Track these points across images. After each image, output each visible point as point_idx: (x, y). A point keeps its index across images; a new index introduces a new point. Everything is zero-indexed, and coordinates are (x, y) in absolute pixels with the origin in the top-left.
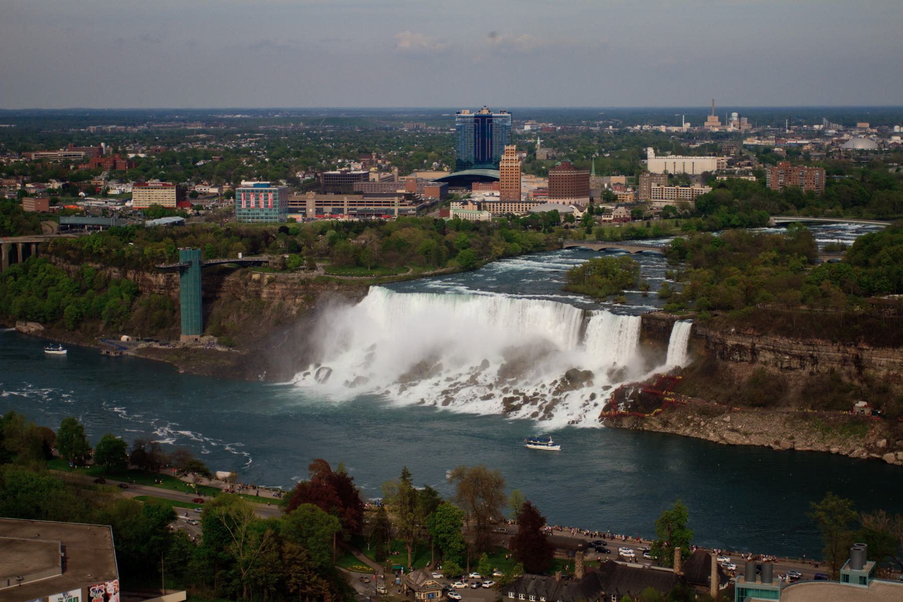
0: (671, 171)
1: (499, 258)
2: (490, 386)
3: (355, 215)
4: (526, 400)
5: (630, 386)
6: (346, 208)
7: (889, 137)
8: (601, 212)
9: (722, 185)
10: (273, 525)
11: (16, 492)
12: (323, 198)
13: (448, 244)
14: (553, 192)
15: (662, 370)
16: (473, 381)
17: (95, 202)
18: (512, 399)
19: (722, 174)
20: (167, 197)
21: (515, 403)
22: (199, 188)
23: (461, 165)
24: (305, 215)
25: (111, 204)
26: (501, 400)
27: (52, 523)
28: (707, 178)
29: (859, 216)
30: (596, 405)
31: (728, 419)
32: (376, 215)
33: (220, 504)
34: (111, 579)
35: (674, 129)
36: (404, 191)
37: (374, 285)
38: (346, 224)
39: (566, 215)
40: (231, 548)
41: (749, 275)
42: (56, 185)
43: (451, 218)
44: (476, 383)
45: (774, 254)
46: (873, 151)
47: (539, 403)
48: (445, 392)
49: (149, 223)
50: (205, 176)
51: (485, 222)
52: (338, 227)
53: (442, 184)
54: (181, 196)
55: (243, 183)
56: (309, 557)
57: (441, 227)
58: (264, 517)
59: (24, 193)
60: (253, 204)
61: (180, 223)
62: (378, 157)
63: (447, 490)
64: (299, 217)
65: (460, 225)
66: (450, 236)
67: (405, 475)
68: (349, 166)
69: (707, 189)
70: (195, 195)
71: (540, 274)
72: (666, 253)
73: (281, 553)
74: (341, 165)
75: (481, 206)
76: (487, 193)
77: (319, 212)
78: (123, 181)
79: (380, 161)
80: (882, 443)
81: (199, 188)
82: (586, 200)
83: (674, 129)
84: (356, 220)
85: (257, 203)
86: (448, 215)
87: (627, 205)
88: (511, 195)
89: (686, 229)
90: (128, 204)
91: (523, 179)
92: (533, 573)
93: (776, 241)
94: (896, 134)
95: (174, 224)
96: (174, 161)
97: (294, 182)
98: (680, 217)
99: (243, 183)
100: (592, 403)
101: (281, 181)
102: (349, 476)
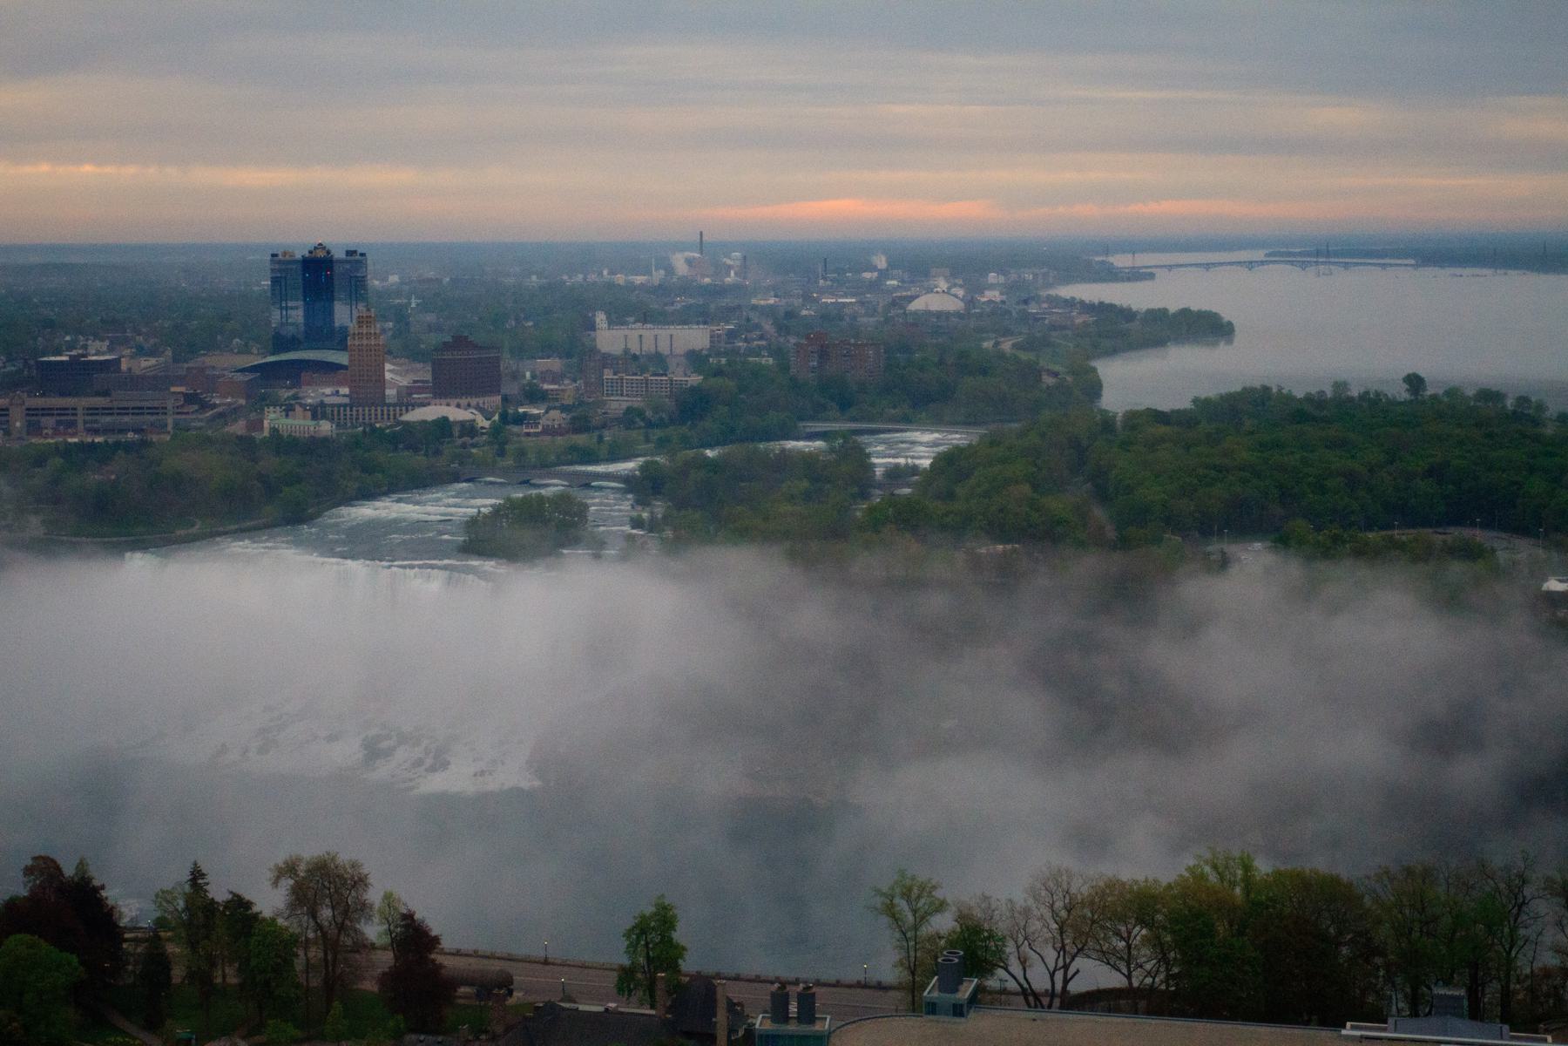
0: (634, 348)
1: (349, 500)
3: (96, 432)
6: (80, 419)
7: (981, 292)
8: (521, 419)
9: (719, 372)
12: (40, 402)
14: (443, 388)
19: (719, 354)
21: (385, 744)
28: (695, 359)
29: (937, 422)
32: (136, 431)
35: (639, 279)
38: (81, 447)
39: (462, 423)
41: (766, 519)
45: (805, 484)
46: (958, 314)
51: (325, 440)
52: (67, 451)
53: (250, 376)
63: (270, 901)
65: (282, 444)
67: (197, 875)
68: (85, 347)
69: (695, 379)
72: (630, 484)
74: (70, 348)
75: (318, 412)
76: (328, 391)
77: (34, 428)
79: (140, 339)
87: (564, 409)
89: (662, 444)
91: (388, 366)
93: (808, 460)
94: (992, 287)
98: (650, 425)
102: (96, 883)
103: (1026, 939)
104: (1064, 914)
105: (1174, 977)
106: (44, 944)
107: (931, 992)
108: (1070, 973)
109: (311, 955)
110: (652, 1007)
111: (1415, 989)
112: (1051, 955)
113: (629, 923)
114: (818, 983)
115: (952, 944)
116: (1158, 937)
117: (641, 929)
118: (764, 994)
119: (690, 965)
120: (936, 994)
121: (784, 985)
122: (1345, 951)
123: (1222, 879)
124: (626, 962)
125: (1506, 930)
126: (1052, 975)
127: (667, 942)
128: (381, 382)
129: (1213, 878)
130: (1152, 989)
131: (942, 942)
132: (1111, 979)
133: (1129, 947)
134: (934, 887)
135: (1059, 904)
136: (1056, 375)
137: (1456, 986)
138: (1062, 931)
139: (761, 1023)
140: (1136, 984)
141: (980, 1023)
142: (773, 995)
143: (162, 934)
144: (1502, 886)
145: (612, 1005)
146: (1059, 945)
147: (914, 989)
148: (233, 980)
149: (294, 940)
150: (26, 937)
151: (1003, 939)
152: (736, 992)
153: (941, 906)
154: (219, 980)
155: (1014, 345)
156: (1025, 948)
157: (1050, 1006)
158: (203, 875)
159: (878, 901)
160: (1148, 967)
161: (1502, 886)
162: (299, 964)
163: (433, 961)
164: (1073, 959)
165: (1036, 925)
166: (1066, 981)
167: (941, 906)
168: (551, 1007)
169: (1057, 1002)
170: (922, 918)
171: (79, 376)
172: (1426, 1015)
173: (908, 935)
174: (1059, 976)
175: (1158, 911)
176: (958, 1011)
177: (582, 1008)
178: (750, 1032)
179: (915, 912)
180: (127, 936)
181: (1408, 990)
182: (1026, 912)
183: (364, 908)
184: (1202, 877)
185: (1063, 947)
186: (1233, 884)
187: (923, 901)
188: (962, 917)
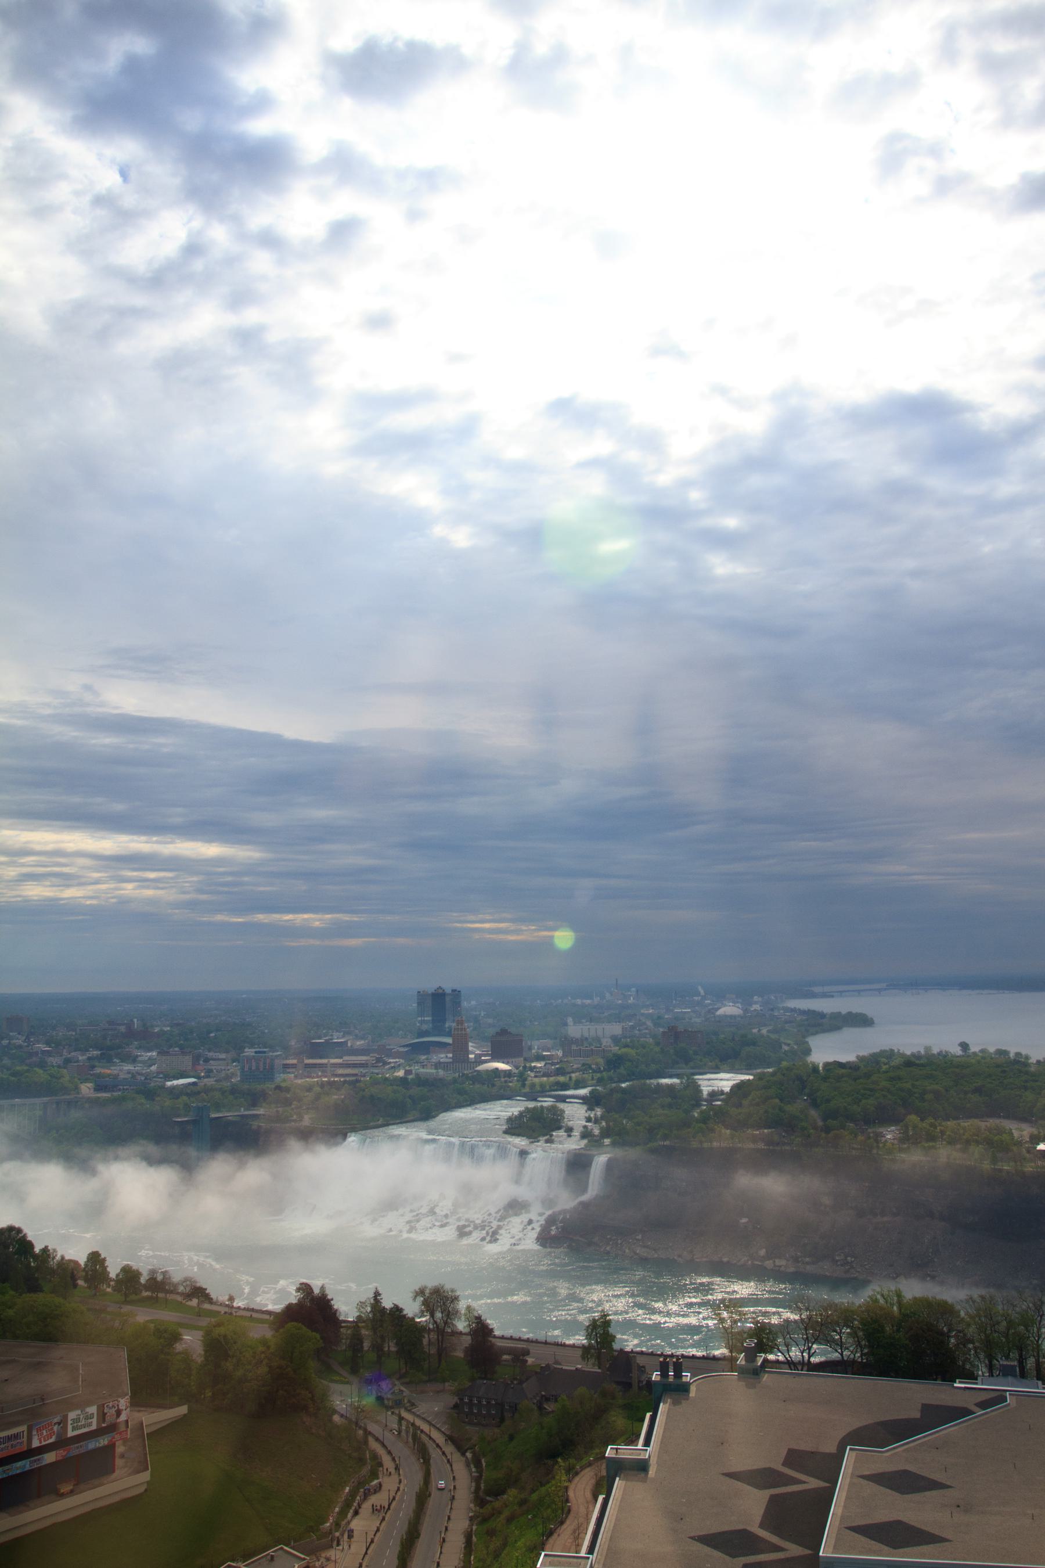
0: (586, 1034)
2: (446, 1216)
3: (336, 1076)
4: (476, 1228)
5: (560, 1213)
7: (751, 1005)
10: (264, 1342)
13: (410, 1097)
15: (585, 1198)
16: (432, 1212)
18: (464, 1226)
19: (625, 1037)
21: (467, 1229)
22: (211, 1054)
23: (422, 1034)
25: (138, 1068)
26: (455, 1226)
28: (616, 1040)
29: (732, 1070)
30: (533, 1229)
31: (639, 1237)
33: (219, 1325)
34: (123, 1396)
35: (588, 1002)
37: (351, 1132)
38: (329, 1083)
41: (651, 1117)
42: (96, 1053)
44: (435, 1213)
45: (669, 1100)
46: (739, 1016)
47: (487, 1228)
48: (408, 1222)
49: (169, 1084)
52: (322, 1085)
53: (406, 1049)
54: (196, 1059)
61: (194, 1084)
63: (412, 1308)
66: (415, 1091)
67: (377, 1294)
68: (332, 1035)
69: (615, 1049)
70: (207, 1060)
72: (584, 1100)
75: (438, 1065)
76: (443, 1056)
78: (150, 1050)
80: (762, 1252)
81: (211, 1054)
83: (588, 1002)
89: (600, 1081)
93: (671, 1087)
94: (756, 1003)
95: (189, 1084)
98: (594, 1071)
99: (246, 1050)
100: (530, 1227)
102: (329, 1297)
105: (865, 1354)
106: (304, 1328)
109: (431, 1337)
110: (599, 1368)
111: (990, 1362)
116: (856, 1333)
122: (953, 1340)
123: (887, 1302)
125: (1035, 1329)
128: (468, 1052)
129: (882, 1301)
130: (854, 1362)
136: (789, 1045)
137: (1012, 1360)
139: (655, 1376)
143: (360, 1324)
144: (1031, 1305)
145: (579, 1366)
148: (393, 1349)
150: (295, 1324)
151: (776, 1334)
154: (386, 1349)
155: (768, 1031)
158: (380, 1295)
161: (1031, 1305)
162: (425, 1341)
163: (491, 1341)
172: (997, 1376)
175: (855, 1319)
177: (564, 1368)
180: (343, 1325)
181: (987, 1362)
183: (457, 1312)
184: (876, 1301)
186: (892, 1305)
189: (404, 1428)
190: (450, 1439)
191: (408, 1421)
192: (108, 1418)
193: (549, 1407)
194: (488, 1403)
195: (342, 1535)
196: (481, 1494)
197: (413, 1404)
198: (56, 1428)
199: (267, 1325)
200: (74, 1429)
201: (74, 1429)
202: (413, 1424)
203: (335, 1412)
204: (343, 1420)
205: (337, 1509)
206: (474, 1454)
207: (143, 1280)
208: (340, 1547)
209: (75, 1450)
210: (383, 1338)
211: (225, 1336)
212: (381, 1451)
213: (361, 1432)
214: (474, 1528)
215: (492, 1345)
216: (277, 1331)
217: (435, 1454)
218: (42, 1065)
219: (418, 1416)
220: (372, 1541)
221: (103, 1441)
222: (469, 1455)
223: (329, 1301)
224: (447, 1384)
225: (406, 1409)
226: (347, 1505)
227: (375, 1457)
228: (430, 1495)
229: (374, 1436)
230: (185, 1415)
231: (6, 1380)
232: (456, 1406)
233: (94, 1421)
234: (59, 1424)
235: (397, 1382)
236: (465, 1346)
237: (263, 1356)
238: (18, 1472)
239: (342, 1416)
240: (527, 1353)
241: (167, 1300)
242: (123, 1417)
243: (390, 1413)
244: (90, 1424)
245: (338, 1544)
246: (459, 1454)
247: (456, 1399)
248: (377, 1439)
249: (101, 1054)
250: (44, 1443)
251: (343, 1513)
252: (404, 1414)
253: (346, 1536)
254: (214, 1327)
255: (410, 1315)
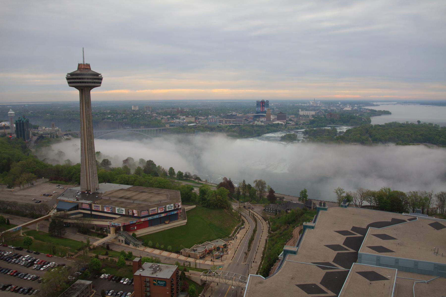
1: (265, 133)
3: (234, 124)
6: (232, 122)
10: (215, 191)
11: (160, 183)
13: (254, 130)
14: (278, 119)
17: (178, 120)
20: (193, 119)
22: (200, 117)
24: (223, 123)
25: (181, 121)
27: (167, 190)
32: (239, 124)
33: (203, 187)
34: (180, 202)
36: (245, 118)
38: (232, 126)
39: (281, 124)
40: (206, 196)
42: (169, 116)
43: (255, 124)
49: (189, 125)
50: (201, 115)
51: (263, 125)
52: (230, 126)
53: (253, 117)
54: (196, 119)
55: (209, 116)
56: (222, 199)
57: (252, 126)
58: (213, 190)
59: (162, 118)
60: (211, 121)
61: (195, 125)
62: (239, 111)
63: (253, 185)
64: (221, 124)
65: (257, 126)
66: (255, 128)
67: (244, 181)
68: (233, 113)
70: (199, 119)
71: (275, 137)
73: (216, 198)
75: (262, 122)
76: (263, 119)
77: (226, 123)
78: (183, 116)
79: (240, 112)
81: (200, 117)
82: (286, 121)
84: (234, 125)
85: (212, 121)
86: (254, 124)
88: (269, 119)
90: (184, 121)
91: (271, 116)
92: (272, 203)
95: (194, 125)
96: (194, 111)
97: (220, 116)
99: (209, 116)
101: (218, 116)
102: (232, 181)
103: (356, 197)
104: (362, 195)
105: (377, 204)
106: (225, 188)
107: (342, 204)
108: (362, 202)
109: (258, 192)
110: (303, 203)
111: (414, 209)
112: (360, 200)
113: (301, 191)
114: (326, 201)
115: (345, 197)
116: (375, 199)
117: (302, 192)
118: (318, 202)
119: (308, 198)
120: (343, 204)
121: (321, 201)
122: (403, 203)
123: (385, 191)
124: (300, 196)
125: (428, 201)
126: (359, 203)
127: (305, 194)
128: (270, 118)
129: (384, 191)
130: (374, 206)
131: (344, 197)
132: (368, 204)
133: (371, 200)
134: (343, 190)
135: (361, 193)
137: (420, 209)
138: (361, 197)
139: (318, 206)
140: (372, 205)
141: (349, 209)
142: (320, 203)
143: (240, 188)
144: (428, 195)
145: (297, 202)
146: (361, 199)
147: (339, 203)
148: (248, 195)
149: (256, 190)
150: (222, 187)
151: (353, 197)
152: (315, 202)
153: (344, 192)
154: (246, 195)
156: (356, 199)
157: (359, 207)
158: (245, 181)
159: (335, 191)
160: (374, 203)
161: (428, 195)
162: (257, 194)
163: (274, 195)
164: (363, 201)
165: (357, 196)
166: (361, 204)
167: (344, 192)
168: (289, 202)
169: (360, 207)
170: (341, 194)
171: (232, 116)
172: (415, 213)
173: (339, 196)
174: (360, 203)
175: (376, 195)
176: (346, 207)
177: (293, 202)
178: (316, 207)
179: (340, 193)
180: (235, 188)
181: (413, 209)
182: (356, 194)
183: (265, 187)
184: (382, 191)
185: (361, 199)
186: (387, 192)
187: (341, 191)
188: (347, 194)
189: (250, 214)
190: (262, 217)
191: (252, 213)
192: (176, 207)
193: (289, 211)
194: (273, 209)
195: (235, 238)
196: (270, 231)
197: (253, 209)
198: (164, 208)
199: (215, 187)
200: (168, 209)
201: (168, 209)
202: (253, 213)
203: (233, 209)
204: (235, 211)
205: (233, 232)
206: (268, 221)
207: (184, 175)
208: (234, 240)
209: (169, 214)
210: (246, 192)
211: (205, 189)
212: (244, 219)
213: (239, 214)
214: (268, 239)
215: (275, 195)
216: (218, 189)
217: (259, 221)
218: (156, 119)
219: (254, 212)
220: (242, 240)
221: (175, 212)
222: (267, 222)
223: (232, 182)
224: (262, 204)
225: (251, 210)
226: (236, 231)
227: (243, 220)
228: (257, 230)
229: (243, 215)
230: (195, 208)
231: (151, 197)
232: (264, 210)
233: (173, 207)
234: (164, 208)
235: (249, 203)
236: (267, 195)
237: (214, 195)
238: (156, 218)
239: (235, 210)
240: (284, 198)
241: (190, 180)
242: (180, 207)
243: (247, 210)
244: (172, 208)
245: (233, 240)
246: (264, 221)
247: (264, 208)
248: (244, 216)
249: (171, 117)
250: (161, 212)
251: (235, 233)
252: (251, 211)
253: (235, 238)
254: (202, 187)
255: (253, 187)
